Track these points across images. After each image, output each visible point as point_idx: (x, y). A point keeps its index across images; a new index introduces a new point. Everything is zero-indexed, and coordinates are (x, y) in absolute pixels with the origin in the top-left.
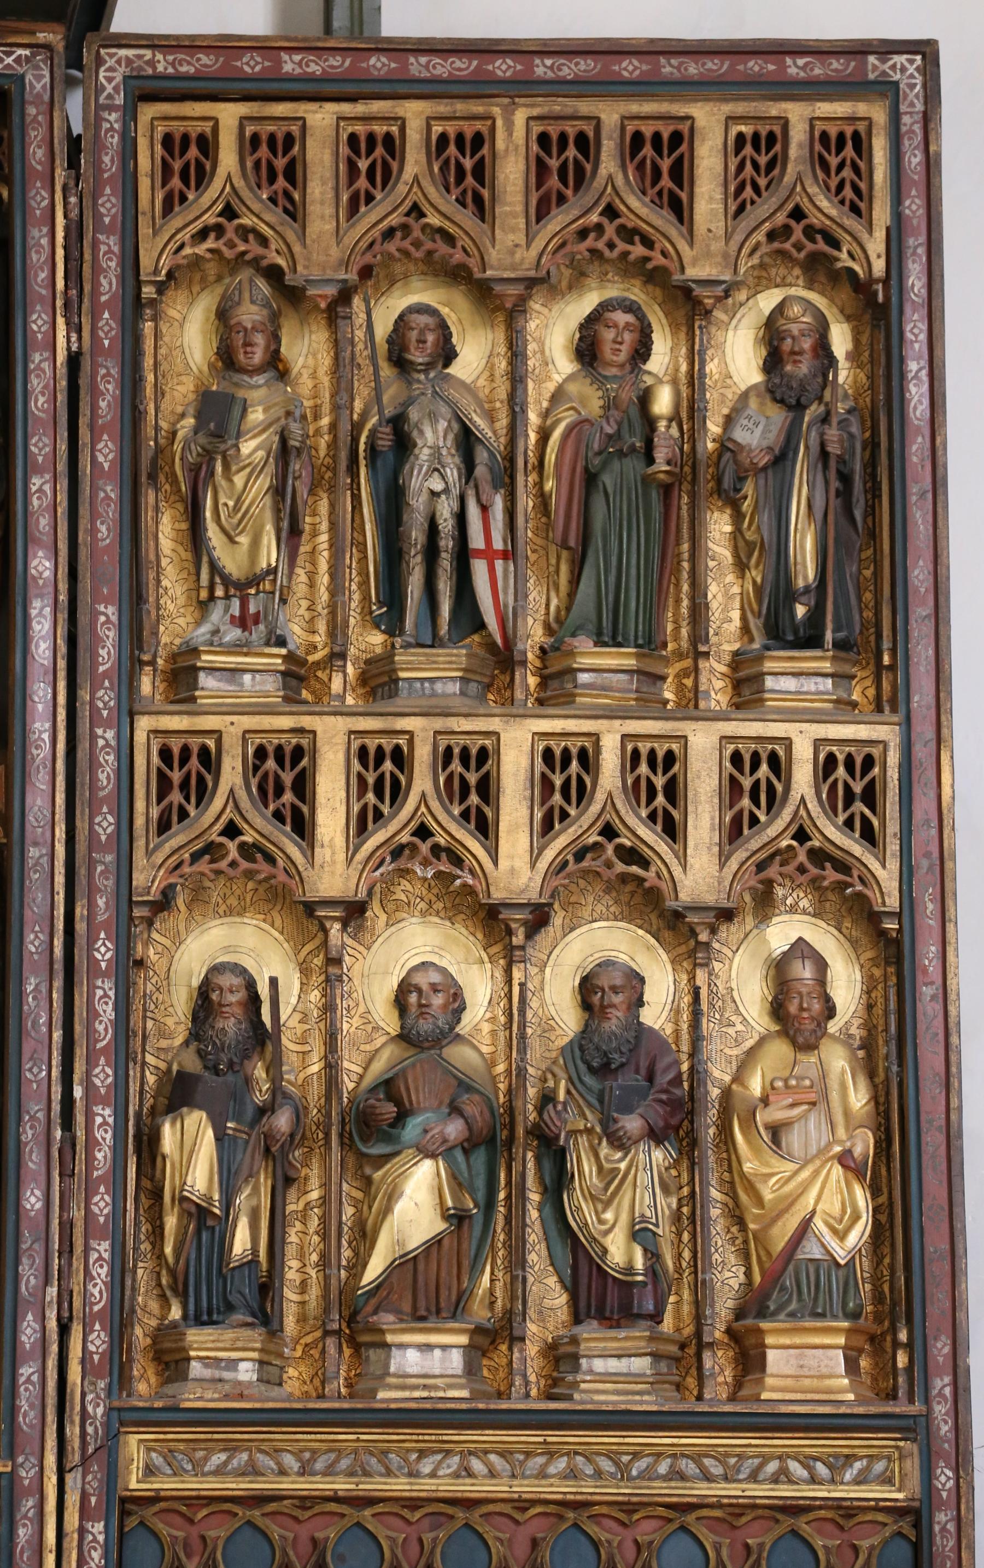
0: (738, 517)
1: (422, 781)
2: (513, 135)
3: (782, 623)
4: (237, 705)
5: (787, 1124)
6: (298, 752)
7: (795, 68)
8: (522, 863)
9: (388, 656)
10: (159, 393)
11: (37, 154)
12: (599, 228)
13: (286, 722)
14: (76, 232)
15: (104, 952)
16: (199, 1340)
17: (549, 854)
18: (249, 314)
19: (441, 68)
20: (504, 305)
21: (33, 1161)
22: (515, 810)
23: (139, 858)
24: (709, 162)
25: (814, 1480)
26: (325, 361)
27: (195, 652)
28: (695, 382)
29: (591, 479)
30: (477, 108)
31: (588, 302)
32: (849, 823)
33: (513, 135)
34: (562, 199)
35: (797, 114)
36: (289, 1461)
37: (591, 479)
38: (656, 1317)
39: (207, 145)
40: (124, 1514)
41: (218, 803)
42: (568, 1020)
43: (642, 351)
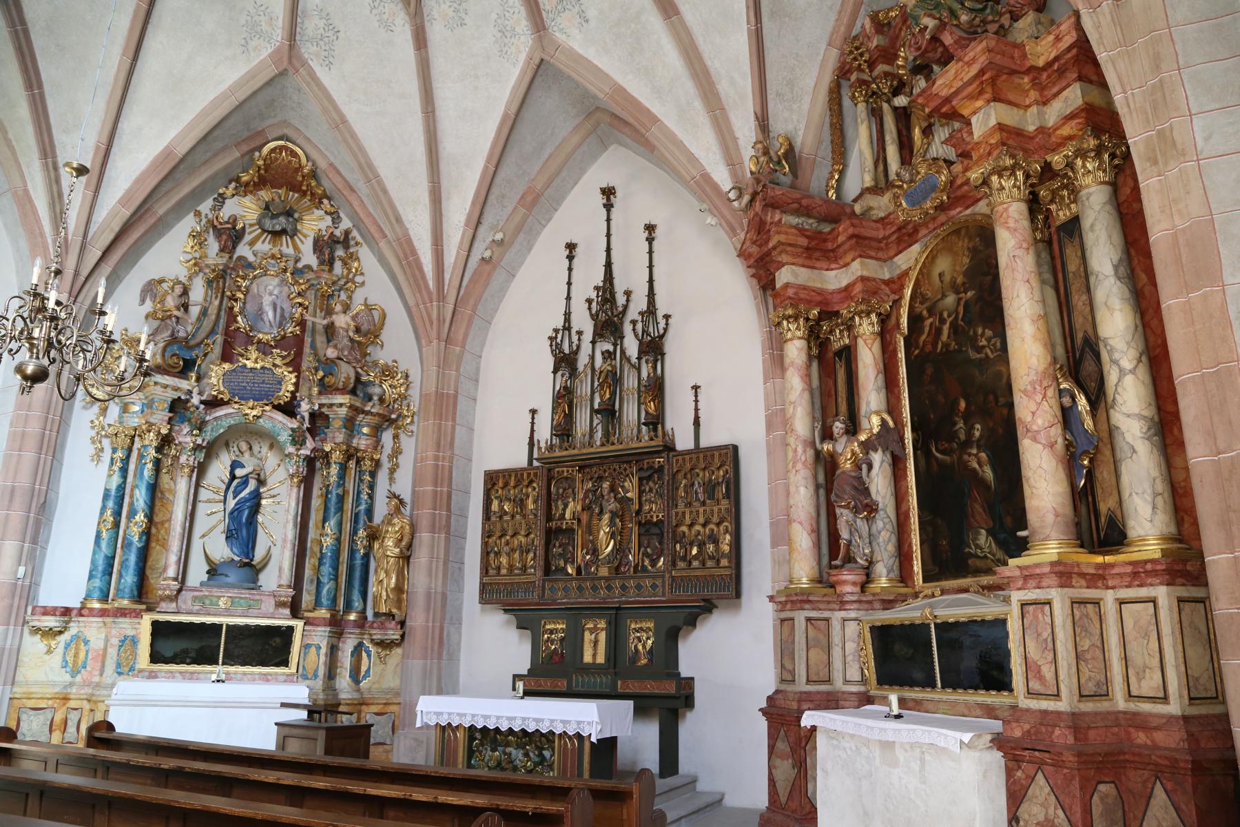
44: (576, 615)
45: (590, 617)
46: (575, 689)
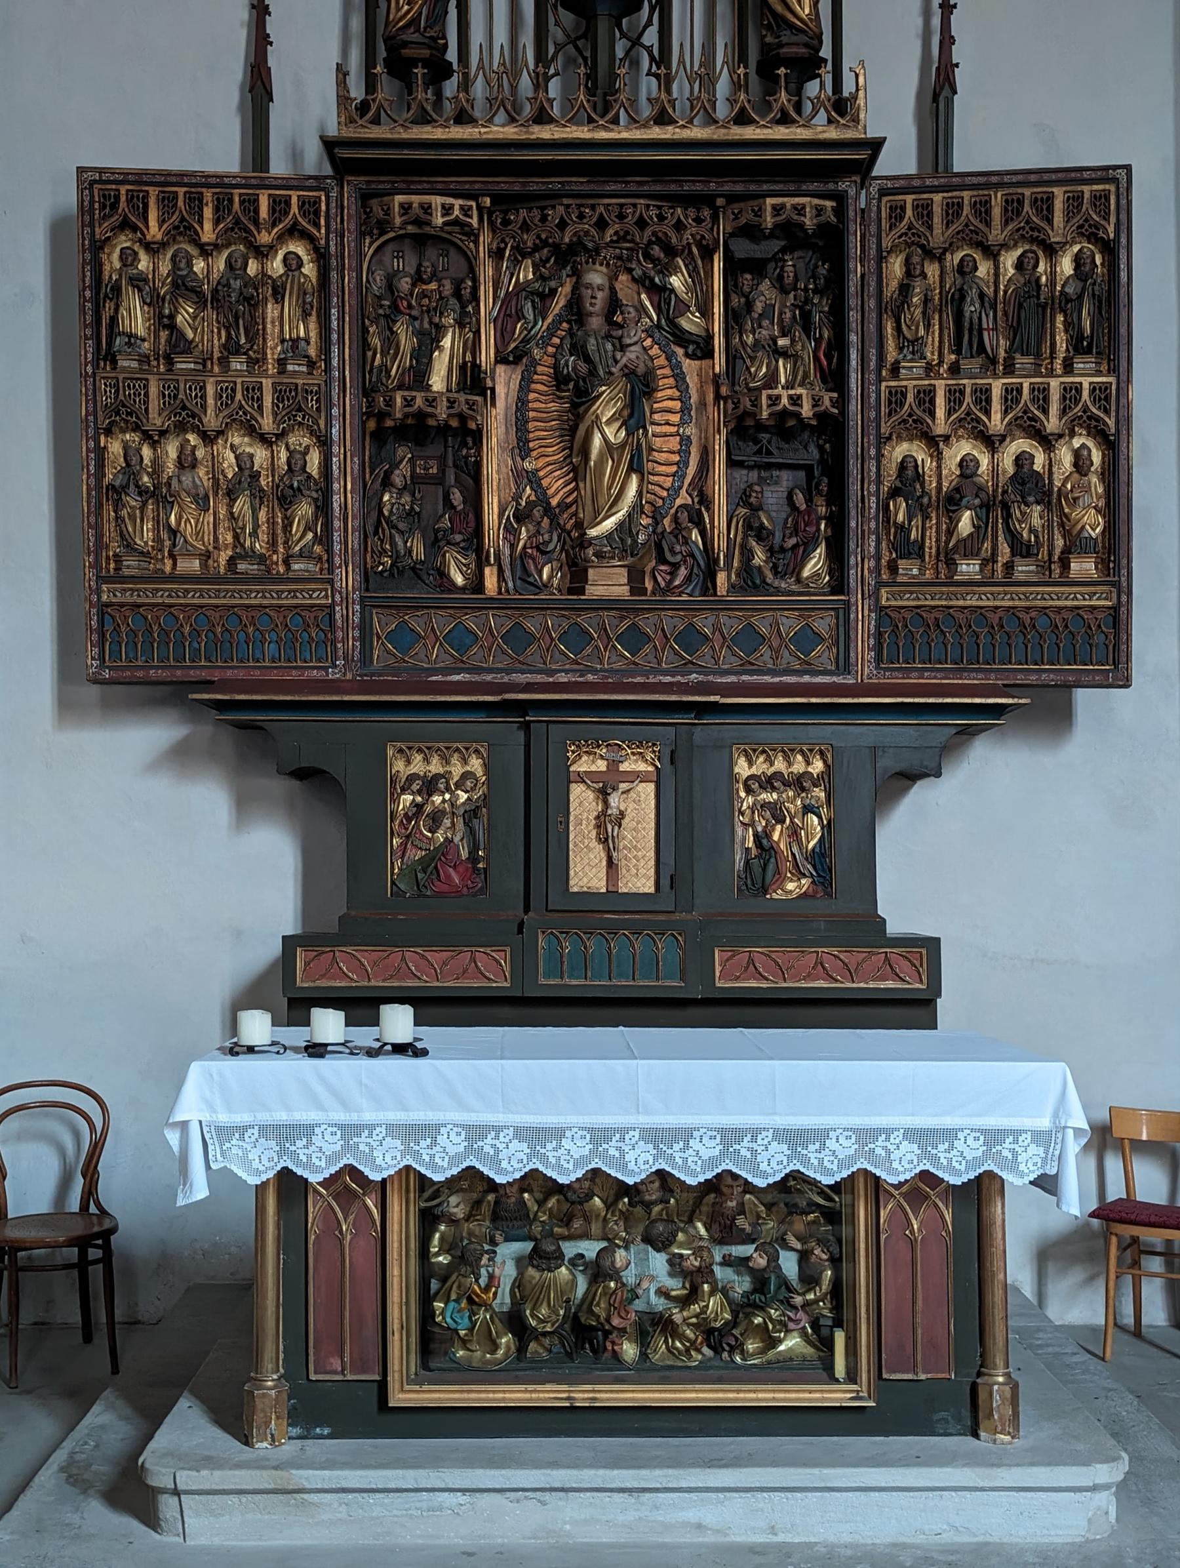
0: (1065, 316)
1: (968, 399)
2: (997, 200)
3: (1079, 346)
4: (911, 380)
5: (1078, 498)
6: (930, 391)
7: (1086, 175)
8: (999, 423)
9: (957, 361)
10: (887, 285)
11: (851, 214)
12: (1023, 228)
13: (927, 382)
14: (863, 236)
15: (873, 452)
16: (902, 564)
17: (1007, 419)
18: (916, 259)
19: (975, 180)
20: (992, 253)
21: (853, 513)
22: (996, 406)
23: (883, 424)
24: (1058, 205)
25: (1084, 599)
26: (937, 273)
27: (899, 363)
28: (1053, 273)
29: (1020, 306)
30: (986, 192)
31: (1019, 251)
32: (1100, 408)
33: (997, 200)
34: (1012, 219)
35: (1086, 189)
36: (928, 596)
37: (1020, 306)
38: (1037, 555)
39: (903, 208)
41: (906, 407)
42: (1011, 470)
43: (1036, 265)
44: (532, 729)
46: (546, 982)
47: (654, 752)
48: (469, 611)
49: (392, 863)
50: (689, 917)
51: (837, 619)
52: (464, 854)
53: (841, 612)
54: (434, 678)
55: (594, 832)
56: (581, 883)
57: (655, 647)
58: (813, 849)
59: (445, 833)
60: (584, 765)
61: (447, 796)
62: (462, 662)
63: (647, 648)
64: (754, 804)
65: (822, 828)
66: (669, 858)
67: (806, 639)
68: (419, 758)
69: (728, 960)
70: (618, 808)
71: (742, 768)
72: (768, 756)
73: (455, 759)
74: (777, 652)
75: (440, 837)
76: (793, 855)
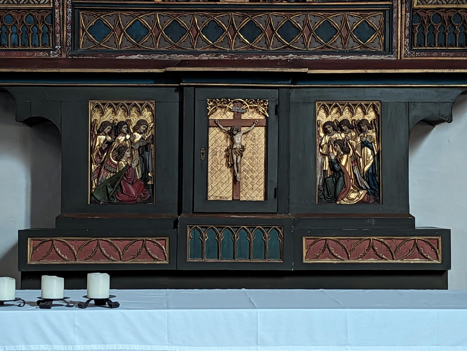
40: (413, 11)
44: (184, 92)
45: (223, 101)
46: (192, 261)
47: (264, 106)
48: (143, 12)
49: (91, 182)
50: (286, 216)
51: (385, 17)
52: (139, 176)
53: (387, 13)
54: (120, 57)
55: (224, 161)
56: (215, 195)
57: (265, 36)
58: (368, 171)
59: (126, 161)
60: (218, 115)
61: (128, 137)
62: (138, 46)
63: (260, 37)
64: (329, 141)
65: (374, 157)
66: (274, 178)
67: (364, 31)
68: (109, 111)
69: (311, 245)
70: (240, 144)
71: (322, 117)
72: (339, 109)
73: (133, 112)
74: (345, 39)
75: (123, 163)
76: (355, 175)
